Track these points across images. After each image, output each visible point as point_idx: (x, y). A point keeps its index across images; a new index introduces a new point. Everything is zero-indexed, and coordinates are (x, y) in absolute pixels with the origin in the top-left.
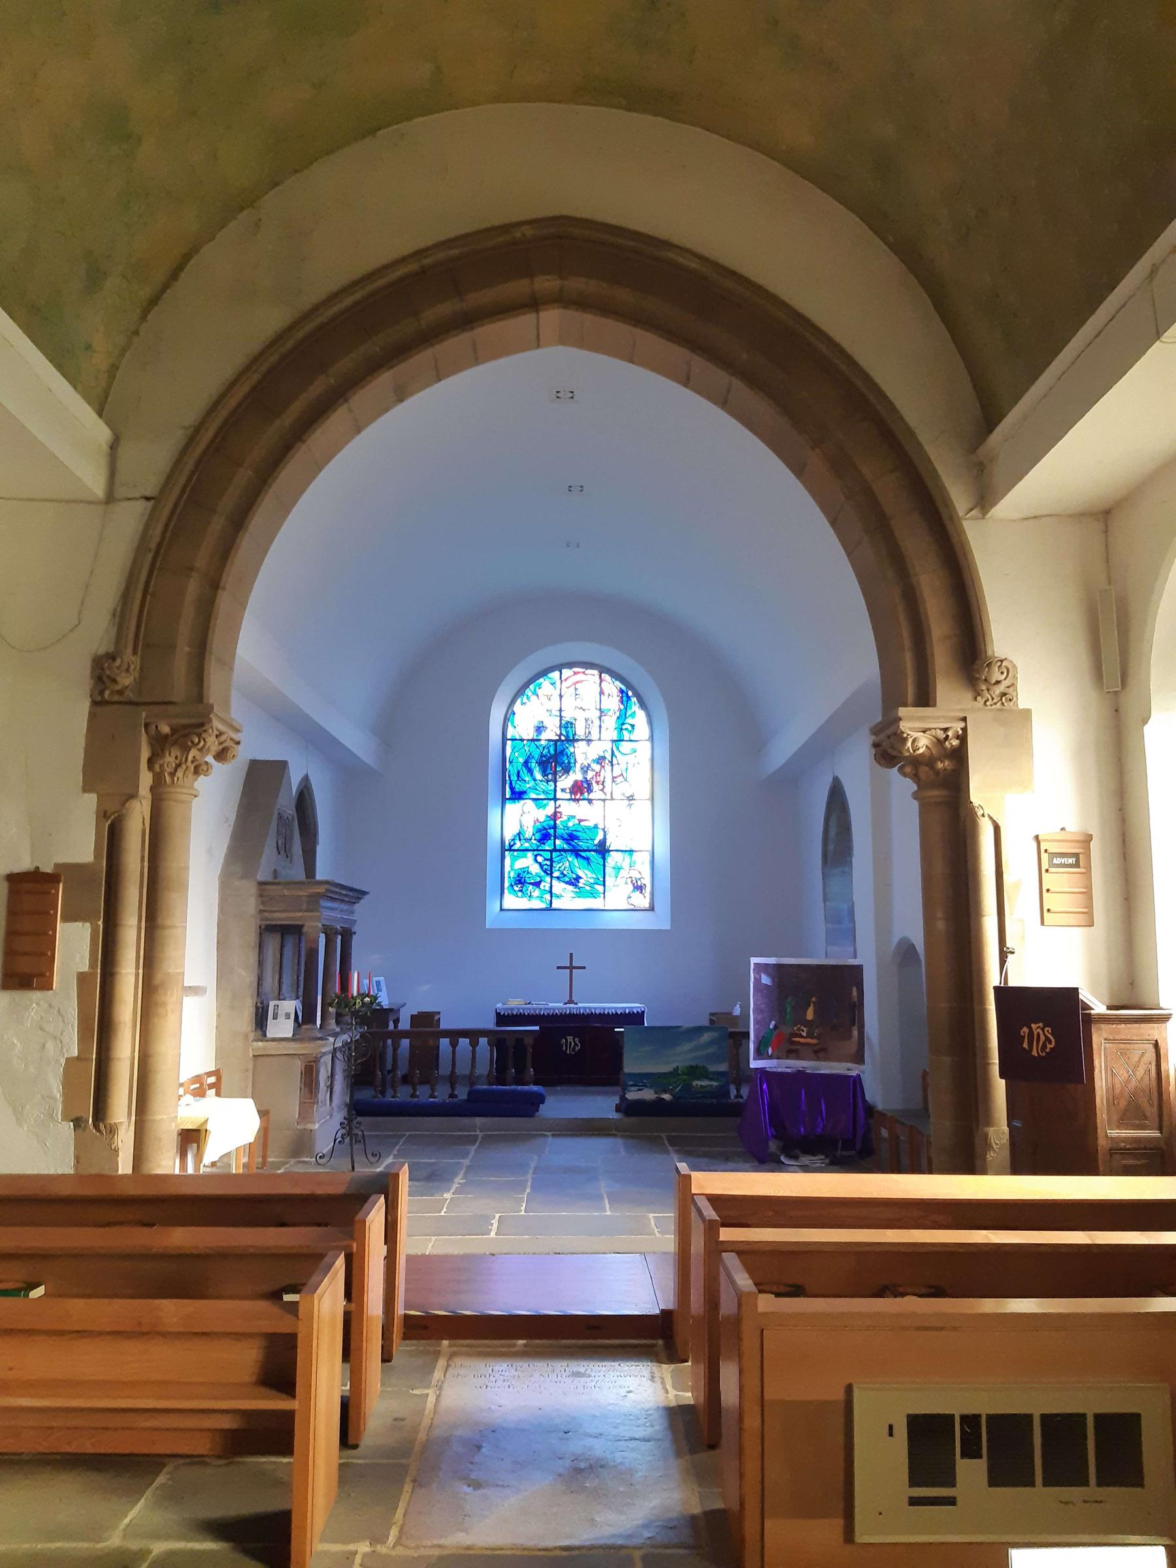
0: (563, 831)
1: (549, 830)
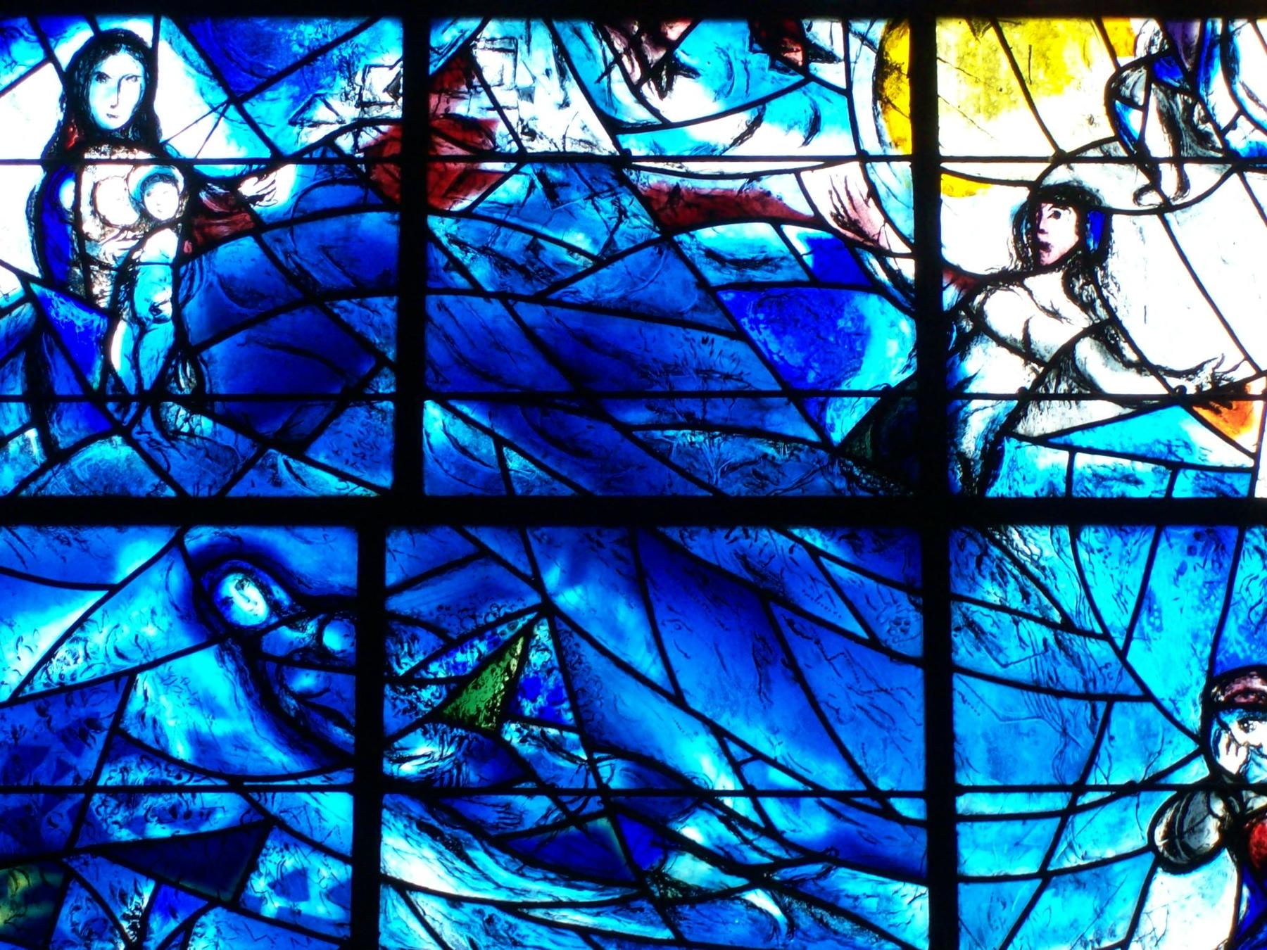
0: (492, 311)
1: (348, 309)
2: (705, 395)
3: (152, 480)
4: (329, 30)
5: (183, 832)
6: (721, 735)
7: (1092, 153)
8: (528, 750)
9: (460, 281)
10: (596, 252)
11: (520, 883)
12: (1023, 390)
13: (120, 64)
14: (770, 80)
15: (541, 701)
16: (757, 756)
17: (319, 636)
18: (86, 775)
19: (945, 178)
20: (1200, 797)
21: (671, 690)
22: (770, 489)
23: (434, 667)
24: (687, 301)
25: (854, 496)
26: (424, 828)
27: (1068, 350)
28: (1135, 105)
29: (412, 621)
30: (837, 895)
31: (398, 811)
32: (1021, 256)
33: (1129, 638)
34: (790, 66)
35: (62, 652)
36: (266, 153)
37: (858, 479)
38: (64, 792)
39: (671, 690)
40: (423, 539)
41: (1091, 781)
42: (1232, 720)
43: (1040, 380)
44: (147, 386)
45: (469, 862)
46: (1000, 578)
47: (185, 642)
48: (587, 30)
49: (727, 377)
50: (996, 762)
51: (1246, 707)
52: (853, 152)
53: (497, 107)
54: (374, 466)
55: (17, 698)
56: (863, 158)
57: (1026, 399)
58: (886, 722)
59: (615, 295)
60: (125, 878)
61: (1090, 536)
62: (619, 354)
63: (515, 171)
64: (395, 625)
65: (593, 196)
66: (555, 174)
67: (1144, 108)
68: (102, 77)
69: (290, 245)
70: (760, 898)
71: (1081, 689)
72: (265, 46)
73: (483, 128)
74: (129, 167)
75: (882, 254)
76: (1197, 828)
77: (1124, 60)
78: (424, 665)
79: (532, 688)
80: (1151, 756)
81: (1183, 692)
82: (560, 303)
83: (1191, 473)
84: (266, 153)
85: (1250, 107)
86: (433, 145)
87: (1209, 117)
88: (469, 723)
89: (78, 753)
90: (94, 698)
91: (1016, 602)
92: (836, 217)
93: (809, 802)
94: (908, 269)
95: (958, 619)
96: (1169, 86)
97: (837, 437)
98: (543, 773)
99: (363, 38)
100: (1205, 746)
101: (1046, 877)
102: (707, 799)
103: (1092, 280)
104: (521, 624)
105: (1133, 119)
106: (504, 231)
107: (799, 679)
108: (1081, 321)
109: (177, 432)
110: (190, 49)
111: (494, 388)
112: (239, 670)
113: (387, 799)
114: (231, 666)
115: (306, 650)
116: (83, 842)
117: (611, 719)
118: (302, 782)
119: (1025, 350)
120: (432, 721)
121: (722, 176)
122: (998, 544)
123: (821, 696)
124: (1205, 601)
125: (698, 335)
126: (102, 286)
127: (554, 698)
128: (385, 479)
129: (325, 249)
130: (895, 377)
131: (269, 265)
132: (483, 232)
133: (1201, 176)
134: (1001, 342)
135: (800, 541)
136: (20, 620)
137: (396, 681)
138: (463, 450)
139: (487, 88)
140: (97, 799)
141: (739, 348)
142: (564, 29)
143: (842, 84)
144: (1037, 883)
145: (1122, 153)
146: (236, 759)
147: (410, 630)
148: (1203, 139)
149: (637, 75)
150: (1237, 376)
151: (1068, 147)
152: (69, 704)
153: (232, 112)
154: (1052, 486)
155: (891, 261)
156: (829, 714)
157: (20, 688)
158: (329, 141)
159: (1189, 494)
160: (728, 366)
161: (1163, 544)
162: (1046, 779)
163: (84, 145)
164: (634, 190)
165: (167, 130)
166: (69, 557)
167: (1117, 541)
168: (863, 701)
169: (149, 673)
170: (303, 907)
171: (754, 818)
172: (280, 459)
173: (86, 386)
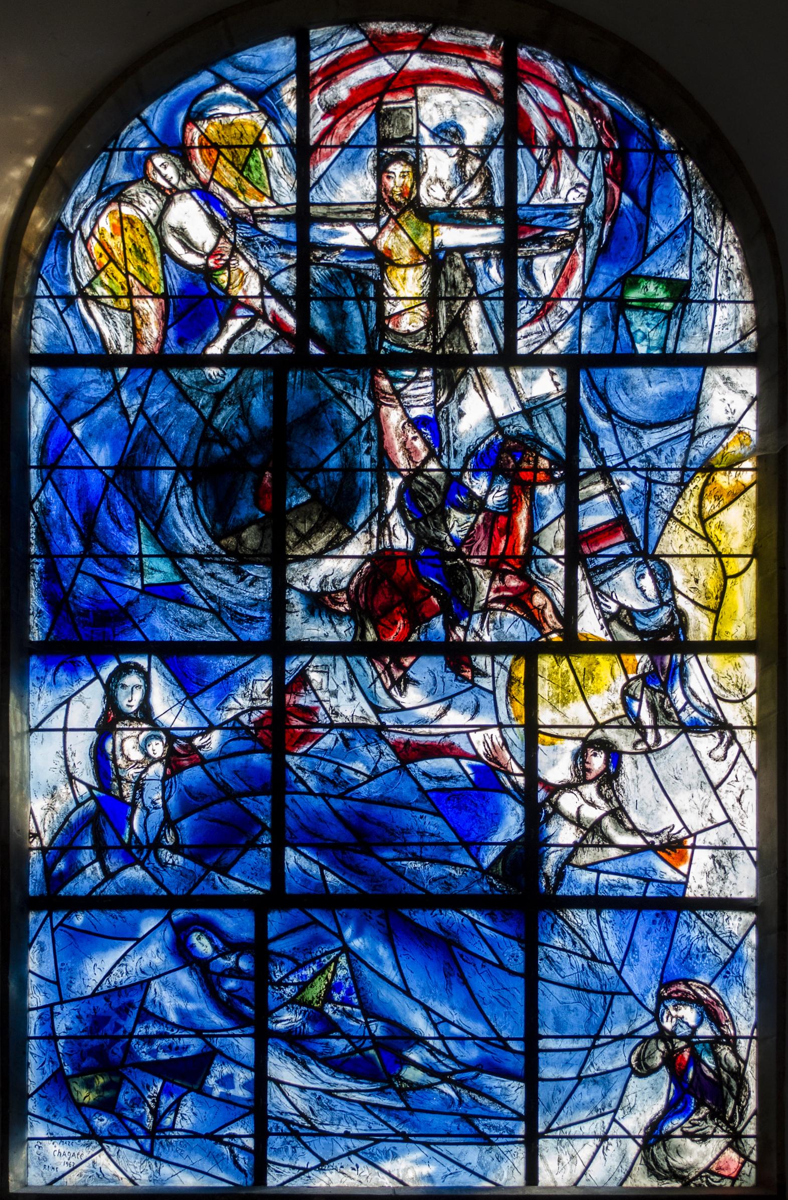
0: (317, 803)
2: (422, 844)
6: (428, 1010)
7: (613, 723)
8: (337, 1017)
9: (302, 788)
11: (333, 1080)
12: (575, 842)
13: (132, 679)
14: (454, 686)
15: (343, 993)
16: (445, 1020)
17: (237, 962)
18: (129, 1030)
23: (291, 977)
24: (413, 797)
25: (493, 895)
26: (288, 1054)
27: (599, 822)
28: (636, 699)
30: (482, 1086)
31: (276, 1046)
34: (465, 679)
35: (115, 971)
36: (206, 725)
37: (495, 886)
38: (119, 1038)
40: (286, 915)
42: (670, 1005)
44: (151, 841)
45: (309, 1070)
46: (562, 934)
47: (173, 966)
48: (364, 661)
49: (432, 835)
50: (558, 1024)
51: (677, 999)
52: (495, 723)
54: (261, 879)
55: (94, 994)
56: (500, 726)
57: (577, 846)
58: (506, 1004)
61: (606, 914)
62: (380, 824)
63: (328, 733)
64: (273, 957)
65: (367, 745)
66: (348, 734)
67: (640, 701)
68: (124, 686)
69: (218, 770)
70: (446, 1088)
71: (599, 989)
72: (203, 671)
73: (312, 711)
74: (137, 732)
75: (508, 774)
77: (631, 676)
78: (287, 976)
79: (338, 987)
80: (631, 1022)
81: (647, 991)
82: (351, 798)
83: (655, 884)
84: (206, 725)
85: (693, 700)
86: (288, 720)
87: (672, 705)
88: (309, 1004)
89: (125, 1019)
90: (131, 993)
91: (569, 947)
94: (521, 781)
95: (541, 954)
96: (653, 689)
97: (485, 865)
98: (344, 1028)
99: (252, 665)
104: (333, 956)
105: (635, 706)
108: (604, 807)
109: (167, 863)
111: (320, 841)
112: (200, 979)
114: (195, 977)
115: (231, 969)
116: (129, 1061)
117: (376, 1002)
118: (230, 1032)
119: (577, 822)
121: (431, 735)
122: (562, 918)
123: (476, 991)
124: (659, 947)
125: (418, 814)
126: (128, 791)
127: (349, 992)
128: (267, 886)
129: (236, 772)
130: (513, 837)
131: (208, 780)
132: (313, 763)
133: (666, 736)
134: (566, 818)
135: (467, 916)
136: (95, 956)
137: (273, 984)
138: (304, 871)
139: (314, 691)
140: (134, 1041)
141: (439, 821)
142: (352, 660)
143: (490, 688)
144: (576, 1081)
145: (628, 723)
146: (198, 1022)
147: (280, 959)
148: (668, 716)
151: (601, 721)
152: (119, 996)
153: (188, 704)
155: (513, 778)
156: (479, 1000)
157: (96, 988)
158: (236, 718)
159: (654, 895)
160: (433, 829)
161: (641, 919)
163: (116, 721)
166: (117, 924)
168: (496, 994)
169: (157, 981)
171: (444, 1050)
172: (216, 876)
173: (122, 841)
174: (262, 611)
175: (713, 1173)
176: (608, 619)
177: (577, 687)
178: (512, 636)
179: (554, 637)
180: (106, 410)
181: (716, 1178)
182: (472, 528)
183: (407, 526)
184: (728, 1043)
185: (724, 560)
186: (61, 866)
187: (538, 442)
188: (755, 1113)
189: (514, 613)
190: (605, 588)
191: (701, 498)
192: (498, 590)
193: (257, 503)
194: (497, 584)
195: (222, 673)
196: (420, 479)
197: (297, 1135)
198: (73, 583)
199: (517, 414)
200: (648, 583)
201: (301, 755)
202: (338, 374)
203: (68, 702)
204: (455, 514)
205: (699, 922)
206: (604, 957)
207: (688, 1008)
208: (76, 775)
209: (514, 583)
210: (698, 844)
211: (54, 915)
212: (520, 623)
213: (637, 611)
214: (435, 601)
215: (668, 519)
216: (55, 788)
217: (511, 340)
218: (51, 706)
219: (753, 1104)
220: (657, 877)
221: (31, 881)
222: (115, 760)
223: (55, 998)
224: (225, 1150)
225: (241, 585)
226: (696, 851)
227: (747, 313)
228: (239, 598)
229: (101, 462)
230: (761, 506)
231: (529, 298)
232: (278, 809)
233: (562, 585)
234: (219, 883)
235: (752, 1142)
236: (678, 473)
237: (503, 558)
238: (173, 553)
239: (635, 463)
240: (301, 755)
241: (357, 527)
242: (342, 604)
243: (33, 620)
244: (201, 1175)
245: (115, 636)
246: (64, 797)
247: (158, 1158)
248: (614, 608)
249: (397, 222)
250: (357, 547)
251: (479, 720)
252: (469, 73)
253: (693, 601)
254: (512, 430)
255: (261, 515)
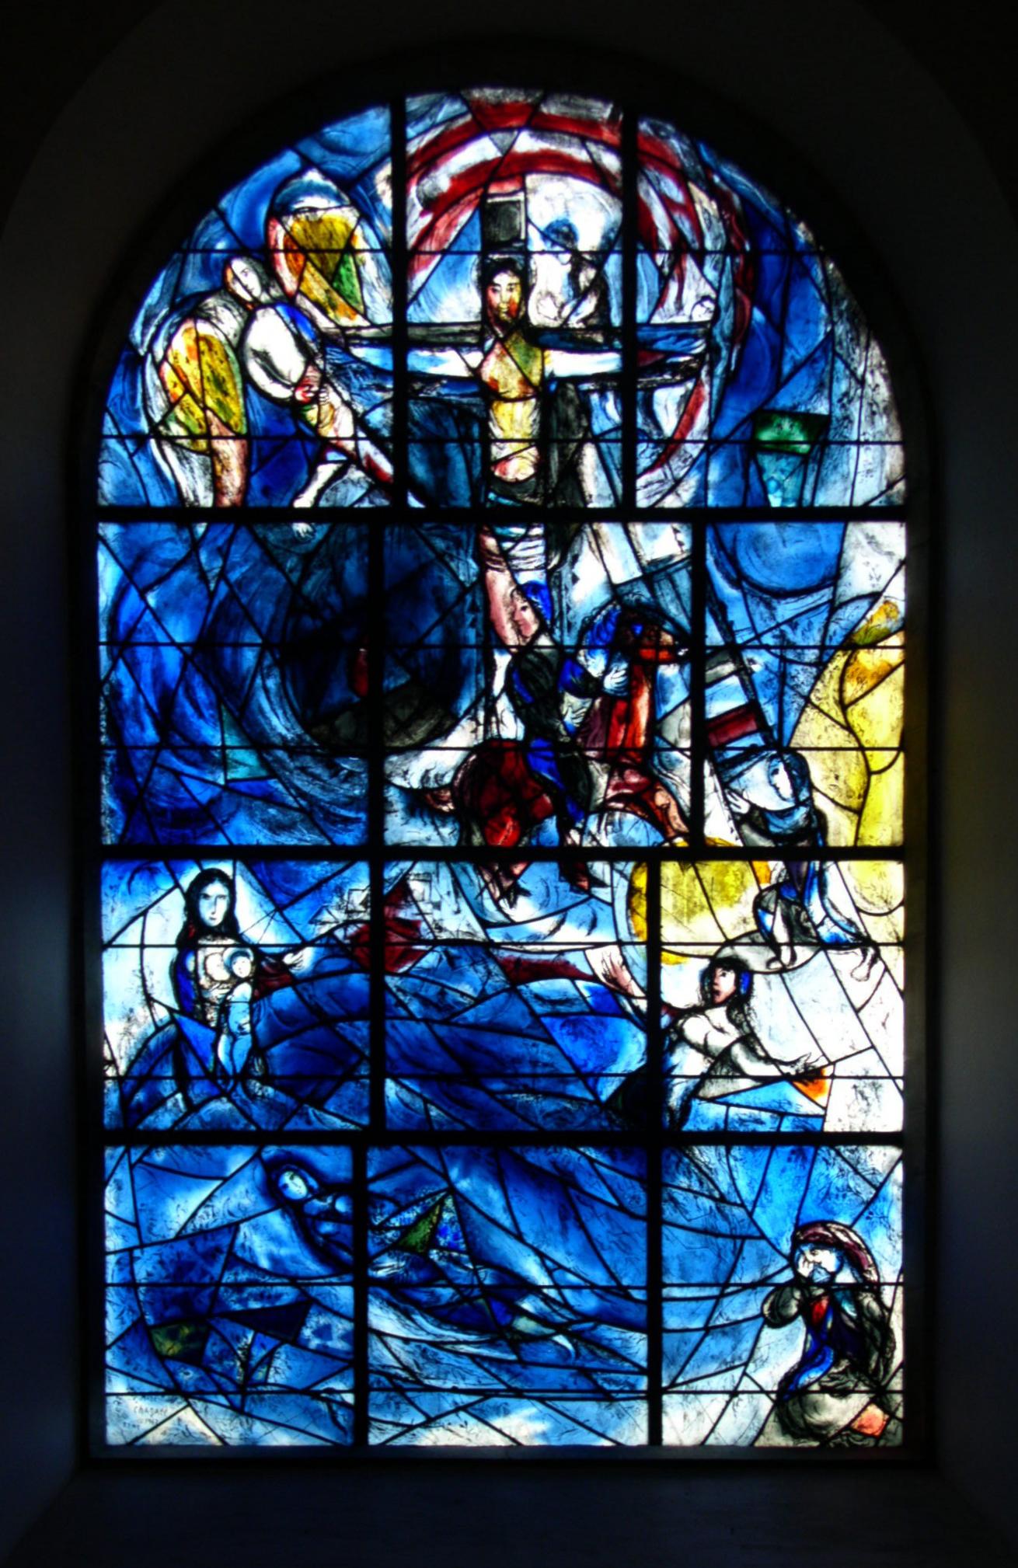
0: (420, 1029)
1: (344, 1027)
2: (534, 1076)
3: (243, 1122)
4: (329, 868)
5: (267, 1305)
6: (542, 1256)
8: (443, 1263)
9: (403, 1013)
10: (475, 995)
13: (215, 889)
14: (570, 897)
15: (449, 1238)
16: (560, 1267)
17: (333, 1204)
18: (217, 1278)
19: (664, 954)
20: (788, 1289)
21: (513, 1230)
22: (569, 1127)
24: (525, 1023)
26: (390, 1304)
27: (727, 1050)
29: (382, 1196)
30: (601, 1338)
31: (377, 1296)
32: (704, 998)
33: (754, 1206)
34: (578, 890)
35: (201, 1212)
36: (298, 941)
38: (205, 1286)
39: (513, 1230)
40: (388, 1154)
41: (732, 1281)
42: (806, 1249)
43: (712, 1068)
45: (413, 1320)
48: (470, 869)
49: (545, 1065)
53: (421, 913)
54: (360, 1114)
55: (179, 1237)
57: (705, 1078)
58: (626, 1249)
59: (486, 1020)
60: (238, 1329)
61: (736, 1152)
62: (489, 1053)
63: (432, 950)
65: (473, 964)
66: (453, 951)
67: (774, 914)
68: (206, 896)
70: (561, 1340)
72: (296, 878)
73: (413, 925)
75: (630, 997)
76: (786, 1305)
77: (764, 886)
78: (388, 1220)
79: (443, 1233)
81: (782, 1234)
82: (457, 1025)
87: (809, 919)
88: (412, 1249)
90: (219, 1237)
91: (696, 1187)
92: (605, 976)
93: (586, 1292)
95: (665, 1196)
97: (604, 1098)
98: (450, 1275)
99: (347, 873)
100: (792, 1264)
101: (708, 1329)
102: (535, 1290)
103: (742, 1011)
104: (438, 1198)
105: (768, 920)
106: (426, 984)
107: (582, 1226)
108: (733, 1033)
109: (255, 1096)
110: (254, 880)
111: (419, 1071)
113: (371, 1289)
116: (218, 1310)
117: (485, 1247)
119: (704, 1049)
120: (393, 1249)
122: (687, 1156)
124: (795, 1186)
125: (530, 1042)
126: (212, 1015)
127: (456, 1237)
128: (365, 1120)
129: (330, 994)
130: (635, 1066)
131: (300, 1004)
133: (803, 953)
134: (693, 1046)
135: (583, 1154)
136: (177, 1195)
138: (406, 1105)
139: (415, 902)
140: (222, 1289)
141: (551, 1049)
143: (608, 899)
145: (761, 940)
146: (293, 1268)
148: (806, 931)
149: (498, 894)
150: (818, 1064)
151: (731, 936)
153: (278, 916)
154: (717, 1126)
157: (180, 1232)
158: (330, 933)
160: (546, 1059)
161: (774, 1157)
162: (709, 1280)
164: (496, 960)
165: (244, 925)
167: (750, 1154)
168: (615, 1239)
170: (330, 1344)
172: (311, 1111)
174: (358, 811)
175: (855, 1432)
176: (739, 820)
177: (704, 900)
178: (632, 840)
179: (680, 842)
180: (182, 576)
181: (859, 1437)
182: (587, 714)
183: (518, 713)
184: (870, 1291)
185: (868, 753)
186: (140, 1096)
187: (664, 616)
188: (901, 1366)
189: (634, 813)
190: (734, 785)
191: (842, 680)
192: (616, 788)
193: (352, 686)
194: (616, 780)
195: (313, 881)
196: (531, 657)
197: (402, 1391)
198: (149, 778)
199: (636, 580)
200: (782, 779)
201: (402, 975)
202: (438, 532)
203: (144, 914)
204: (569, 699)
205: (839, 1159)
206: (734, 1198)
207: (827, 1252)
208: (155, 996)
209: (634, 779)
210: (837, 1073)
211: (133, 1151)
212: (641, 825)
213: (771, 812)
214: (548, 799)
215: (806, 706)
216: (131, 1010)
217: (630, 490)
218: (126, 918)
219: (898, 1356)
220: (793, 1110)
221: (107, 1112)
222: (197, 978)
223: (134, 1242)
224: (323, 1406)
225: (335, 781)
226: (836, 1081)
227: (894, 458)
228: (332, 795)
229: (179, 639)
230: (908, 691)
231: (650, 440)
232: (378, 1036)
233: (687, 781)
234: (313, 1118)
235: (898, 1398)
236: (816, 651)
237: (623, 750)
238: (258, 741)
239: (768, 640)
240: (402, 975)
241: (462, 713)
242: (445, 803)
243: (106, 821)
244: (296, 1433)
245: (195, 838)
246: (141, 1020)
247: (250, 1415)
248: (744, 808)
249: (503, 346)
250: (463, 736)
251: (596, 937)
252: (582, 156)
253: (833, 800)
254: (632, 598)
255: (356, 699)
